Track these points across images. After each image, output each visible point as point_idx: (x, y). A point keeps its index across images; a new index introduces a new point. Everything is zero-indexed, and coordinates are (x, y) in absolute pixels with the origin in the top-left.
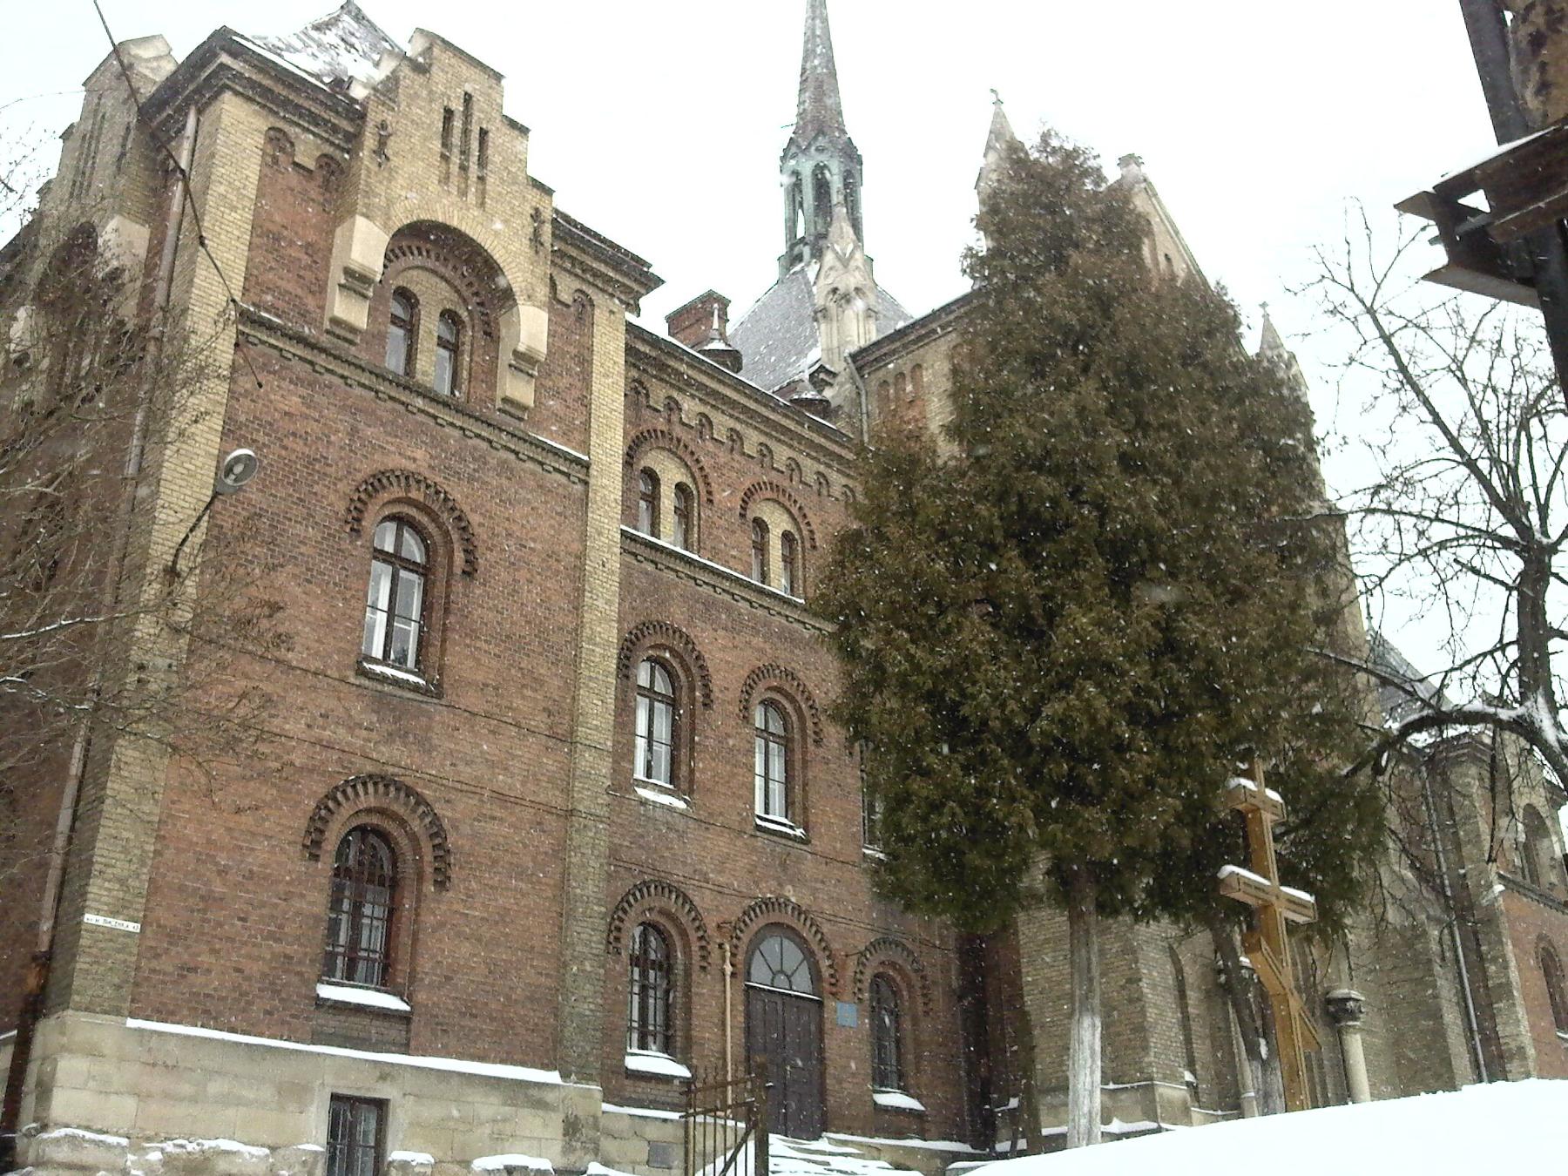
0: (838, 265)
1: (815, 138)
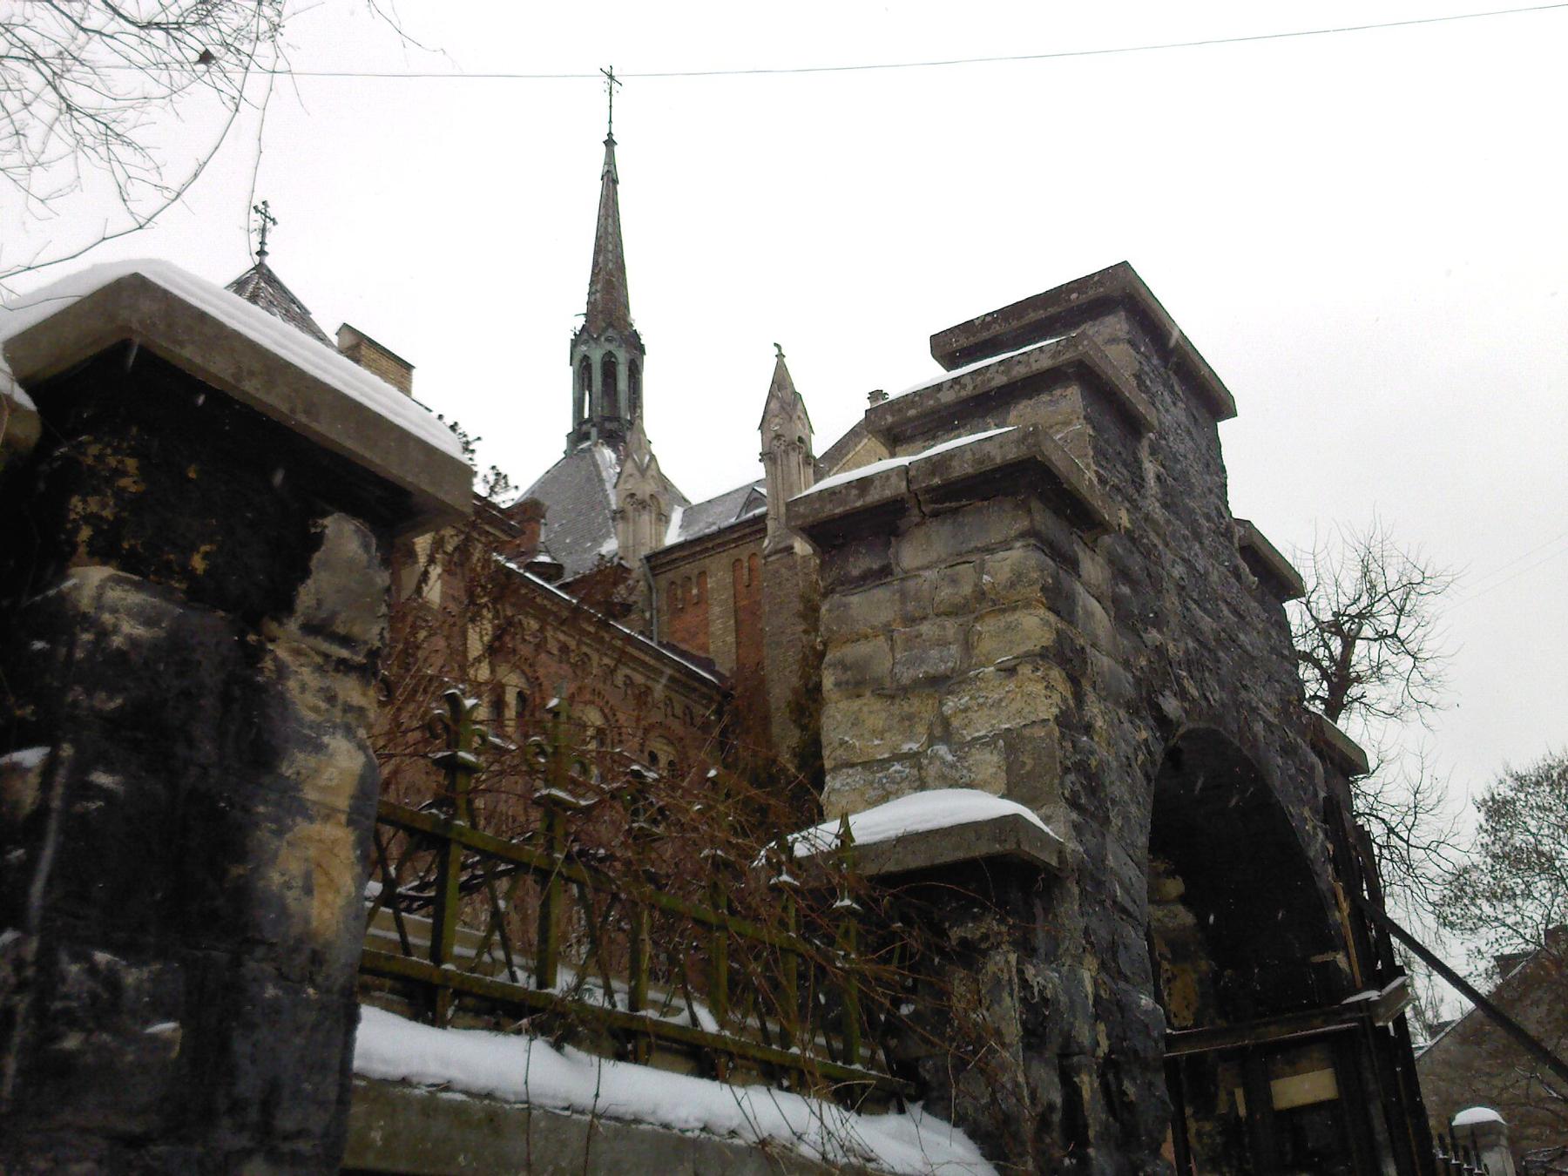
0: (637, 474)
1: (605, 330)
